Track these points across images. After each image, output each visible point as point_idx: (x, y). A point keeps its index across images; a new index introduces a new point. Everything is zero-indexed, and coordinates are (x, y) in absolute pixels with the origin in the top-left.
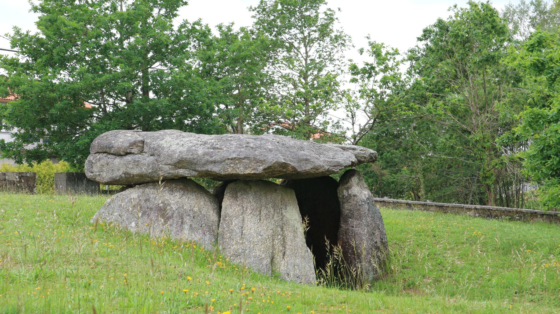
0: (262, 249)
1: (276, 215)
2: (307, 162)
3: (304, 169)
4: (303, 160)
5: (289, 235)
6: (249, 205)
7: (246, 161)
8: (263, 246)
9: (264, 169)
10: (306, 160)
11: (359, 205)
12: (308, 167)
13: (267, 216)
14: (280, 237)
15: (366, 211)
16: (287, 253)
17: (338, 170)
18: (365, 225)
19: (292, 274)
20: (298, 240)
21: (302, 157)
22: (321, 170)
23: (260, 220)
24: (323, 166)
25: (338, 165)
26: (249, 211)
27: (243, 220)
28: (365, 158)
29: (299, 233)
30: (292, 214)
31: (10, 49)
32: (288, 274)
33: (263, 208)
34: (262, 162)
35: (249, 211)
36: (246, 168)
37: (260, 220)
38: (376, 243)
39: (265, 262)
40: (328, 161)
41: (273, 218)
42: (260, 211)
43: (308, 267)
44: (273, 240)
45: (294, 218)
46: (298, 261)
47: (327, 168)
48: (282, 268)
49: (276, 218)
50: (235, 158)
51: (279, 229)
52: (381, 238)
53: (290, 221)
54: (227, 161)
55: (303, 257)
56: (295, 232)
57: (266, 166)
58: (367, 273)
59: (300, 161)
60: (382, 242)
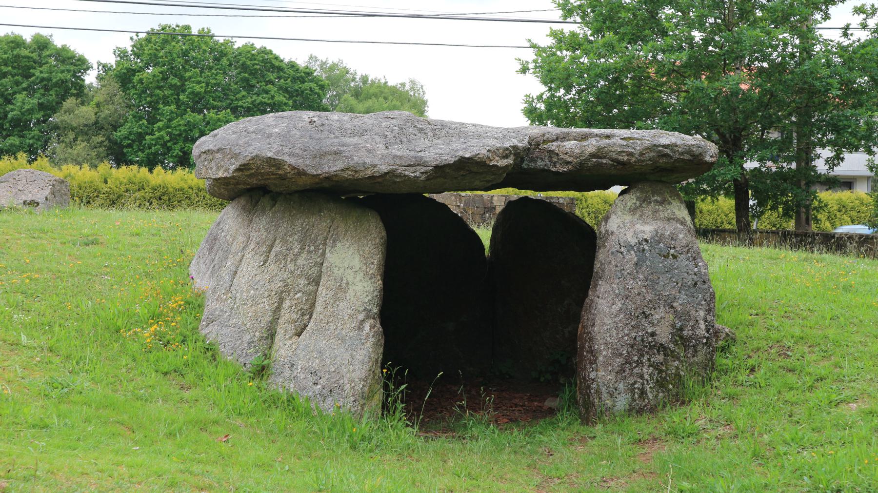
0: (250, 314)
1: (304, 255)
2: (337, 157)
3: (326, 169)
4: (330, 153)
5: (324, 294)
6: (256, 234)
7: (219, 155)
8: (253, 308)
9: (238, 170)
10: (336, 153)
11: (612, 253)
12: (331, 167)
13: (282, 257)
14: (299, 295)
15: (629, 268)
16: (308, 328)
17: (418, 174)
18: (617, 296)
19: (300, 364)
20: (342, 305)
21: (328, 149)
22: (369, 173)
23: (265, 262)
24: (375, 166)
25: (419, 163)
26: (252, 246)
27: (241, 260)
28: (630, 154)
29: (351, 293)
30: (344, 255)
31: (561, 20)
32: (293, 365)
33: (277, 242)
34: (236, 156)
35: (252, 246)
36: (218, 168)
37: (265, 262)
38: (653, 334)
39: (247, 337)
40: (395, 156)
41: (294, 260)
42: (271, 247)
43: (347, 356)
44: (281, 301)
45: (346, 264)
46: (323, 344)
47: (384, 168)
48: (283, 352)
49: (300, 262)
50: (209, 151)
51: (303, 281)
52: (673, 326)
53: (336, 270)
54: (204, 156)
55: (342, 340)
56: (342, 288)
57: (237, 164)
58: (611, 396)
59: (323, 155)
60: (681, 337)
